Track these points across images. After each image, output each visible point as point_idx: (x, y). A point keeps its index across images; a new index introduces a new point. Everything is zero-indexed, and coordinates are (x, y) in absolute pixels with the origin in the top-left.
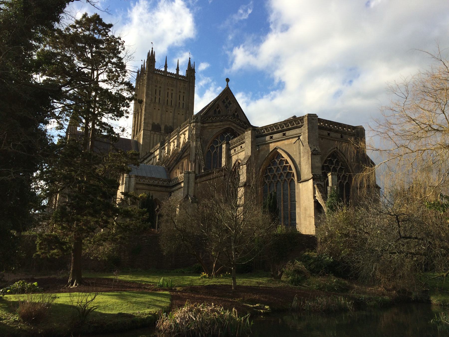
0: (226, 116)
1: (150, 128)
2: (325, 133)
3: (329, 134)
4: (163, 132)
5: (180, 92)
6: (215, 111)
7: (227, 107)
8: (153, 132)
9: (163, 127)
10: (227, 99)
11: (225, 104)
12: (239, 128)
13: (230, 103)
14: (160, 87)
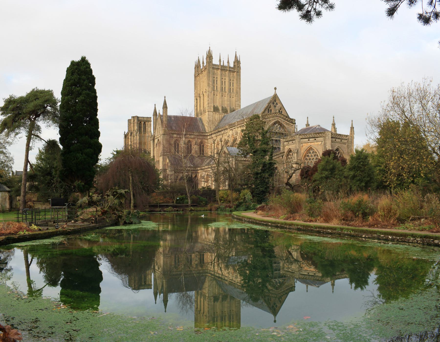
0: (275, 113)
1: (212, 110)
2: (334, 139)
3: (335, 140)
4: (221, 112)
5: (230, 80)
6: (269, 110)
7: (275, 106)
8: (215, 113)
9: (220, 108)
10: (275, 101)
11: (274, 105)
12: (283, 120)
13: (277, 104)
14: (217, 78)
